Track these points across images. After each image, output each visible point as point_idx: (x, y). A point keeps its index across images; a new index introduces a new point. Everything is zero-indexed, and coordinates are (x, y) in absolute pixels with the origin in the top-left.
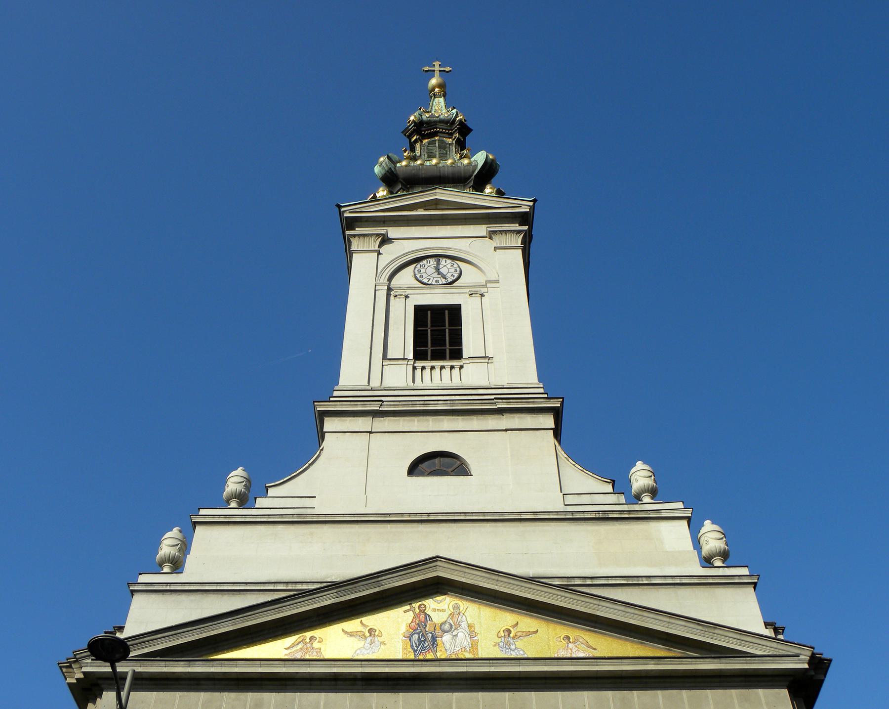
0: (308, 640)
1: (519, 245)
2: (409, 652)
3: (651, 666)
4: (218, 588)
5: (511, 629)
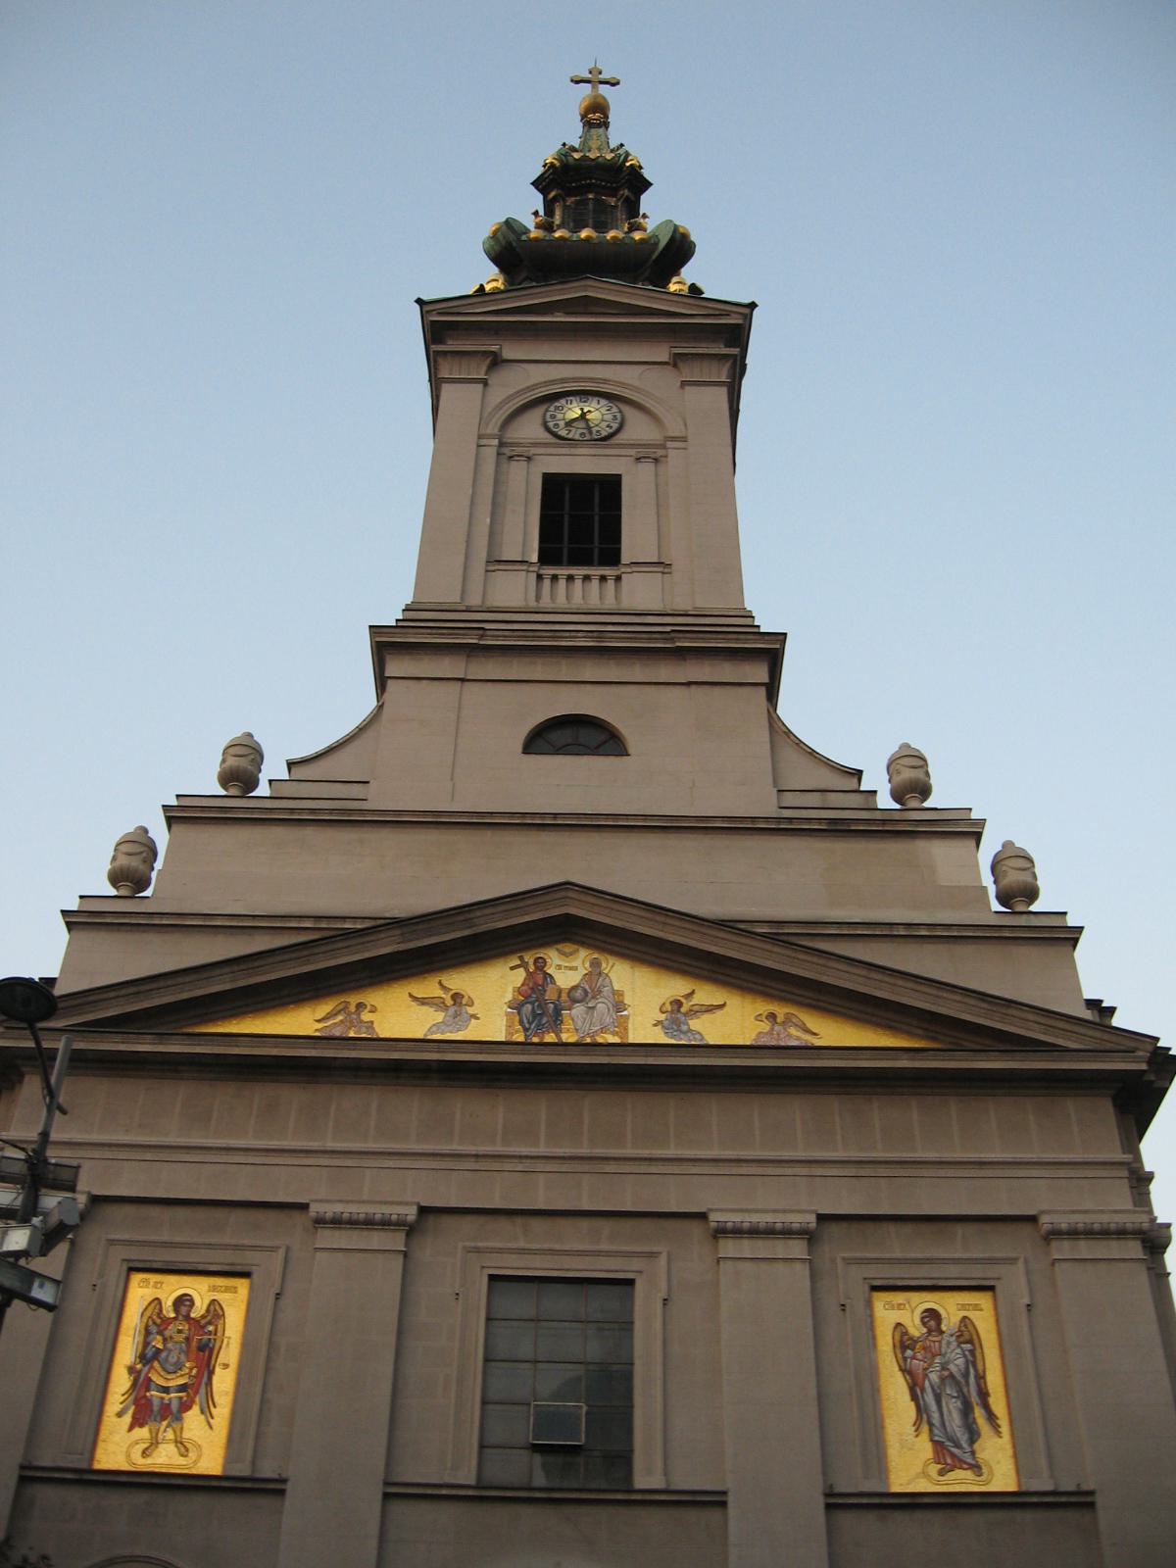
0: (353, 1008)
1: (723, 379)
2: (517, 1032)
3: (904, 1063)
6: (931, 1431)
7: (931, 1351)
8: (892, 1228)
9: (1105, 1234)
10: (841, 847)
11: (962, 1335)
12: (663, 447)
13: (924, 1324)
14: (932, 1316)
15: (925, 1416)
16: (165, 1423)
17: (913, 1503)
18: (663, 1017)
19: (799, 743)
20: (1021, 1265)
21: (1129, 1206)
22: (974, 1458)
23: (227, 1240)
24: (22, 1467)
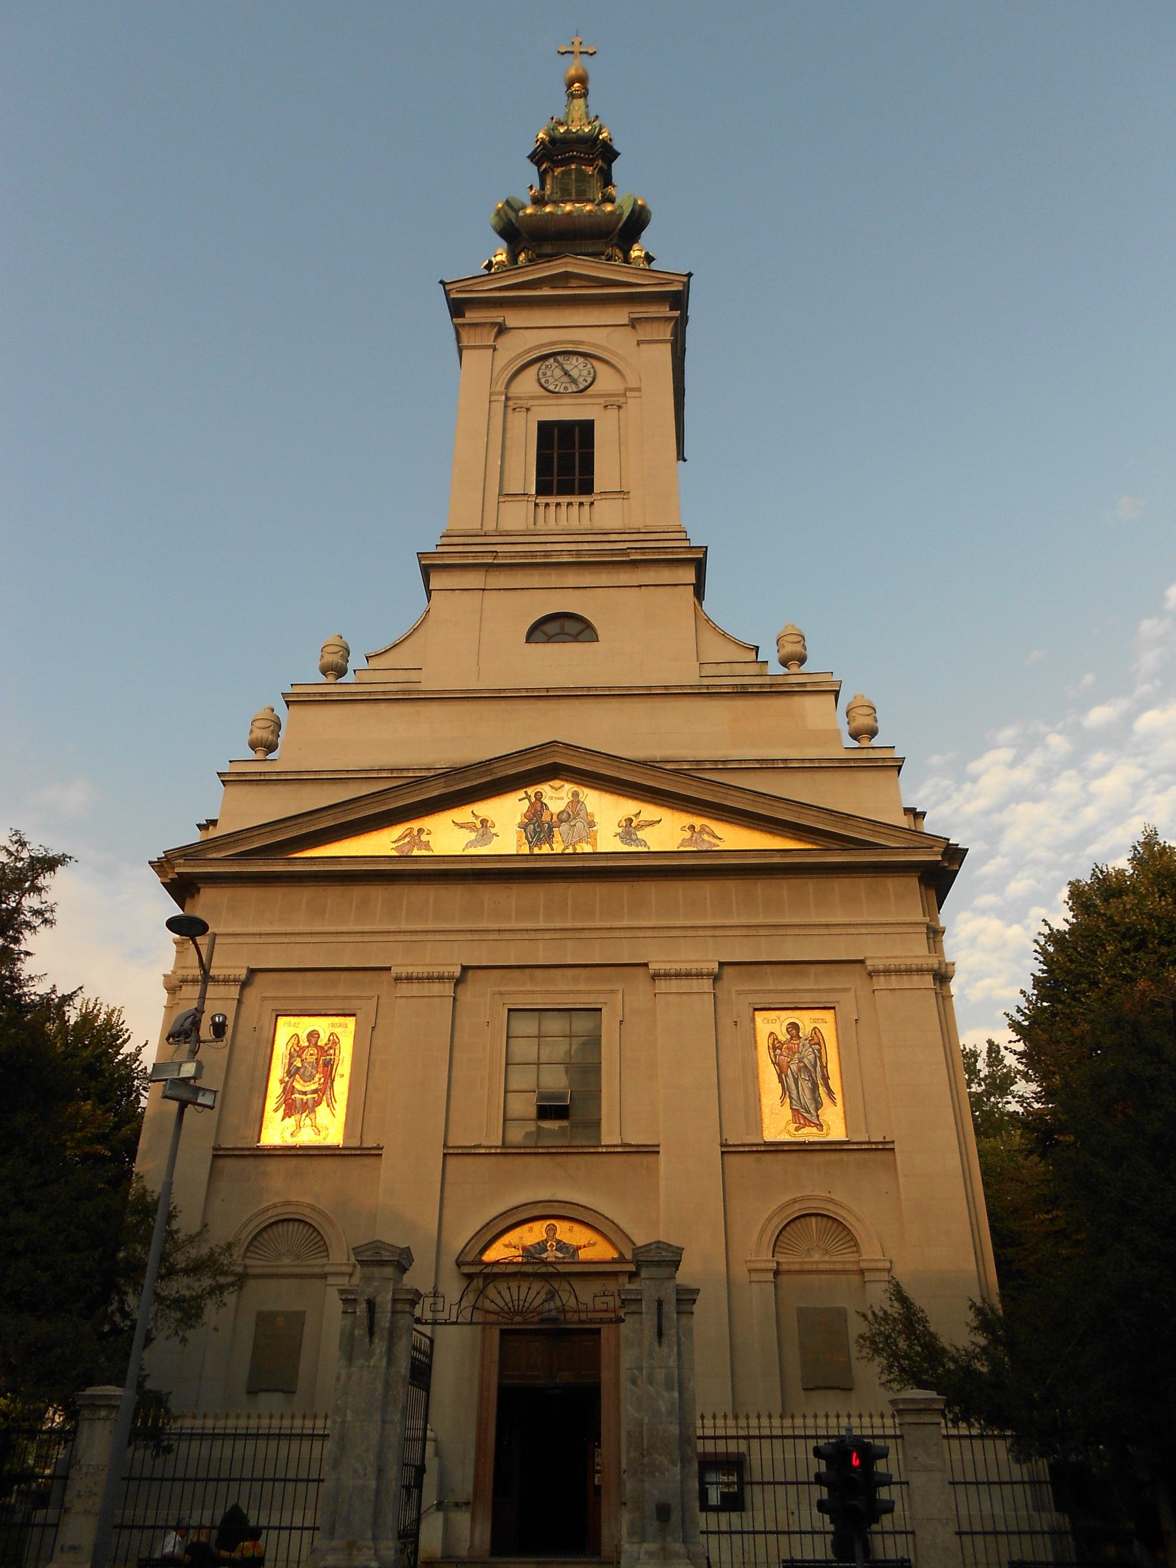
0: (415, 833)
2: (524, 844)
4: (317, 777)
5: (633, 818)
6: (791, 1102)
7: (792, 1051)
8: (768, 968)
9: (909, 971)
10: (741, 704)
11: (813, 1040)
12: (625, 395)
13: (788, 1032)
14: (794, 1027)
15: (787, 1093)
16: (304, 1115)
17: (777, 1148)
18: (620, 830)
19: (715, 628)
20: (852, 992)
21: (926, 953)
22: (818, 1120)
23: (340, 993)
24: (215, 1149)
